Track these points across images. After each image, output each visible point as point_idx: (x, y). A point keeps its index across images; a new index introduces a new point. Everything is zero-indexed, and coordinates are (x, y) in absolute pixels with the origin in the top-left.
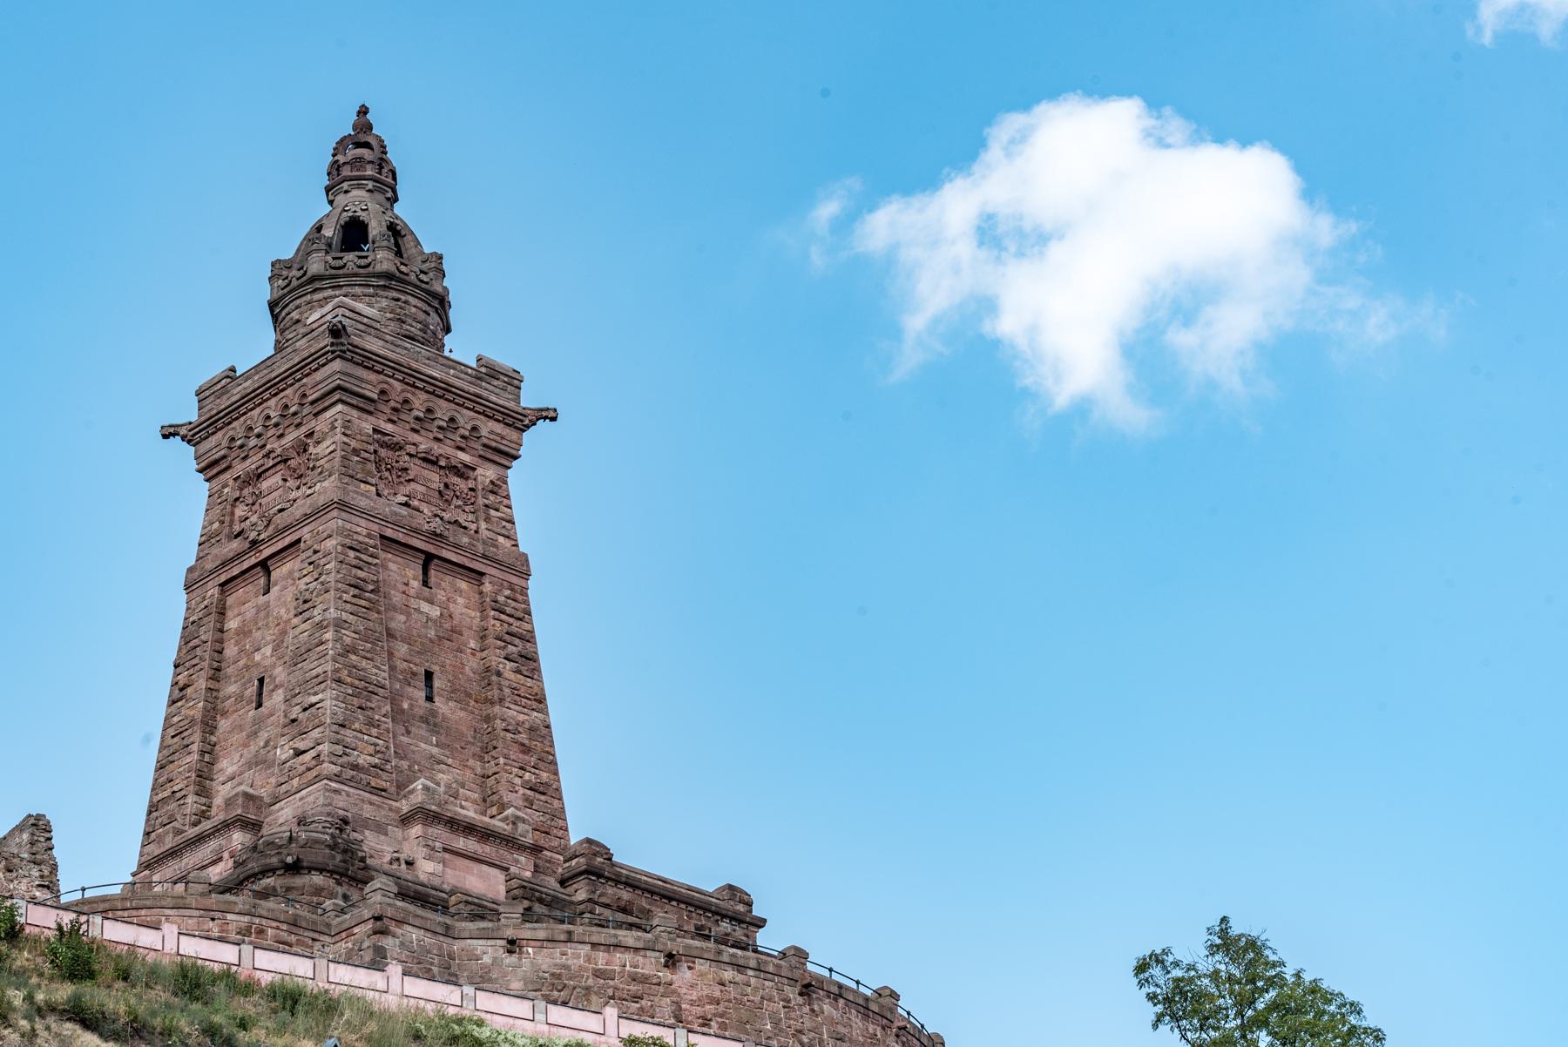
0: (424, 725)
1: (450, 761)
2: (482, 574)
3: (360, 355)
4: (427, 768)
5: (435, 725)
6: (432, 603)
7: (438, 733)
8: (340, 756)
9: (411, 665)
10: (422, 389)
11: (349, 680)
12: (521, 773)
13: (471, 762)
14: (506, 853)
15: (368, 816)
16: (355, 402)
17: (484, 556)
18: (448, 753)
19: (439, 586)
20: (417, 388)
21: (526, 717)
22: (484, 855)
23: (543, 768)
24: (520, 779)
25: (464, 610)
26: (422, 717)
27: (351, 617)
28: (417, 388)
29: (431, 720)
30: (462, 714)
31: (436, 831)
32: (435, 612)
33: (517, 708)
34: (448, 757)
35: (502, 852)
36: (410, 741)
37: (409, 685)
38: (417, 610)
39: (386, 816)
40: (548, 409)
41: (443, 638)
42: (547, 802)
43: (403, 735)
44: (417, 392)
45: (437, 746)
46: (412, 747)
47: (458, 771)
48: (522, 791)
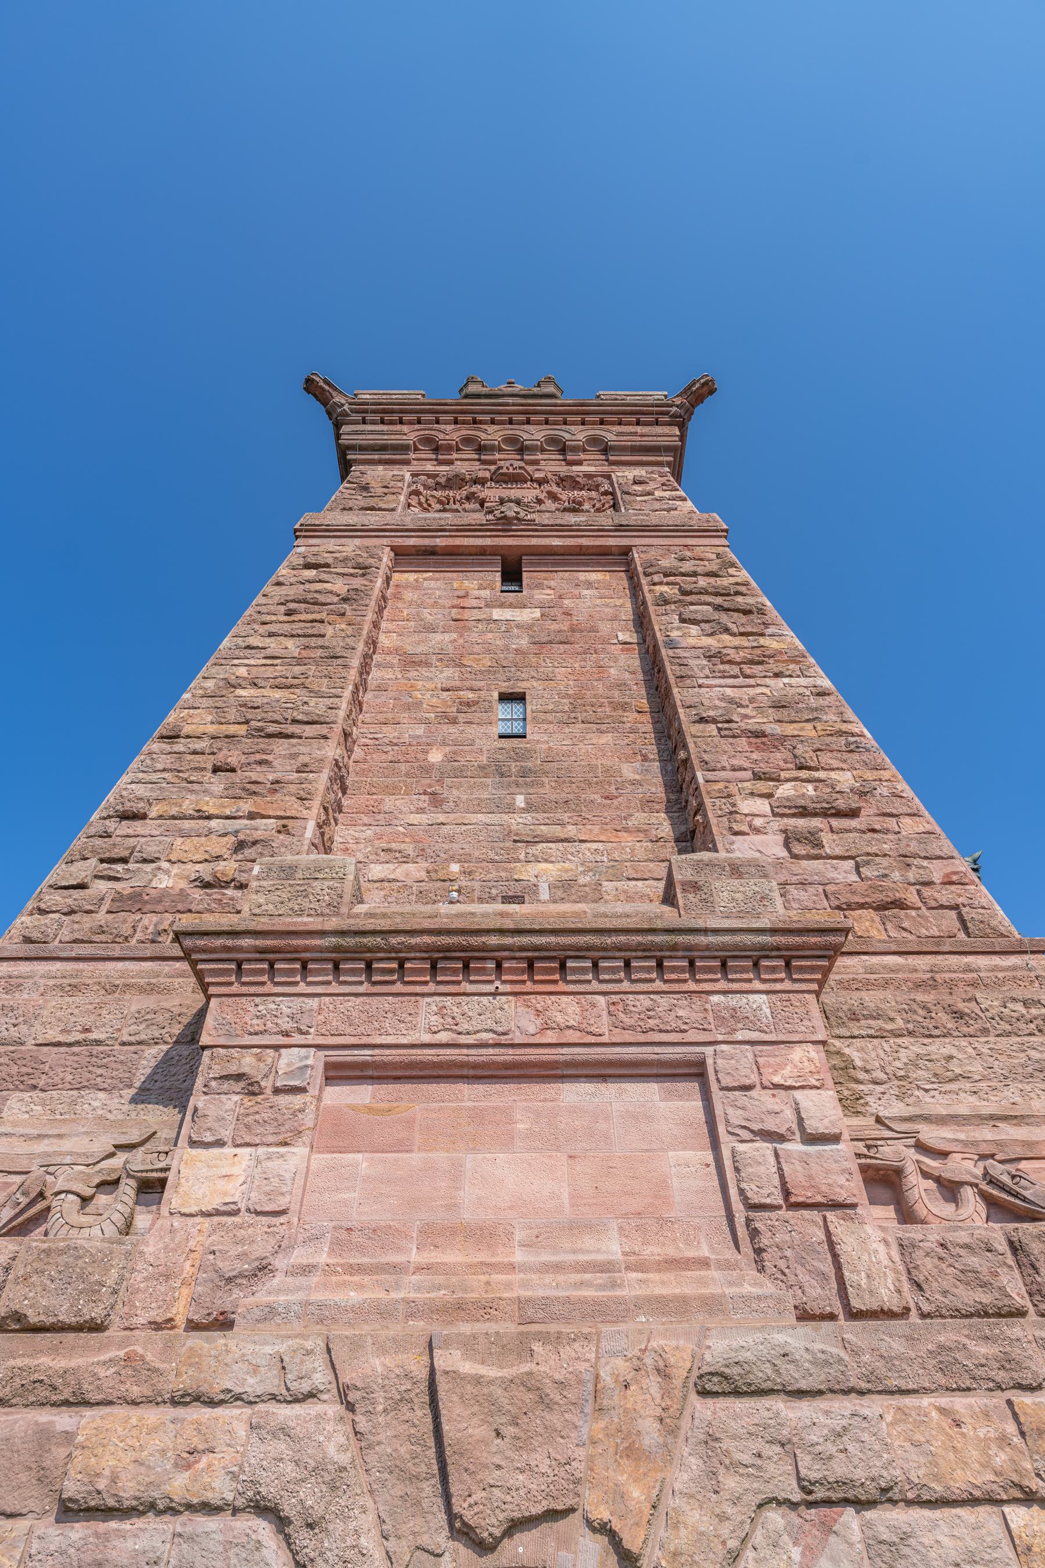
0: (489, 781)
1: (571, 831)
2: (626, 551)
3: (374, 412)
4: (492, 861)
5: (524, 773)
6: (525, 607)
7: (532, 784)
8: (82, 886)
9: (461, 693)
10: (493, 422)
11: (211, 729)
12: (762, 787)
13: (639, 818)
14: (664, 1002)
15: (53, 1034)
16: (376, 457)
17: (620, 528)
18: (565, 817)
19: (539, 586)
20: (481, 422)
21: (759, 690)
22: (550, 1037)
23: (835, 764)
24: (766, 802)
25: (598, 602)
26: (482, 768)
27: (268, 640)
28: (481, 422)
29: (514, 767)
30: (607, 738)
31: (286, 1006)
32: (526, 615)
33: (730, 681)
34: (563, 825)
35: (645, 1001)
36: (441, 818)
37: (454, 722)
38: (490, 620)
39: (140, 1017)
40: (693, 384)
41: (551, 642)
42: (874, 831)
43: (421, 811)
44: (485, 427)
45: (529, 808)
46: (445, 829)
47: (595, 846)
48: (777, 824)
